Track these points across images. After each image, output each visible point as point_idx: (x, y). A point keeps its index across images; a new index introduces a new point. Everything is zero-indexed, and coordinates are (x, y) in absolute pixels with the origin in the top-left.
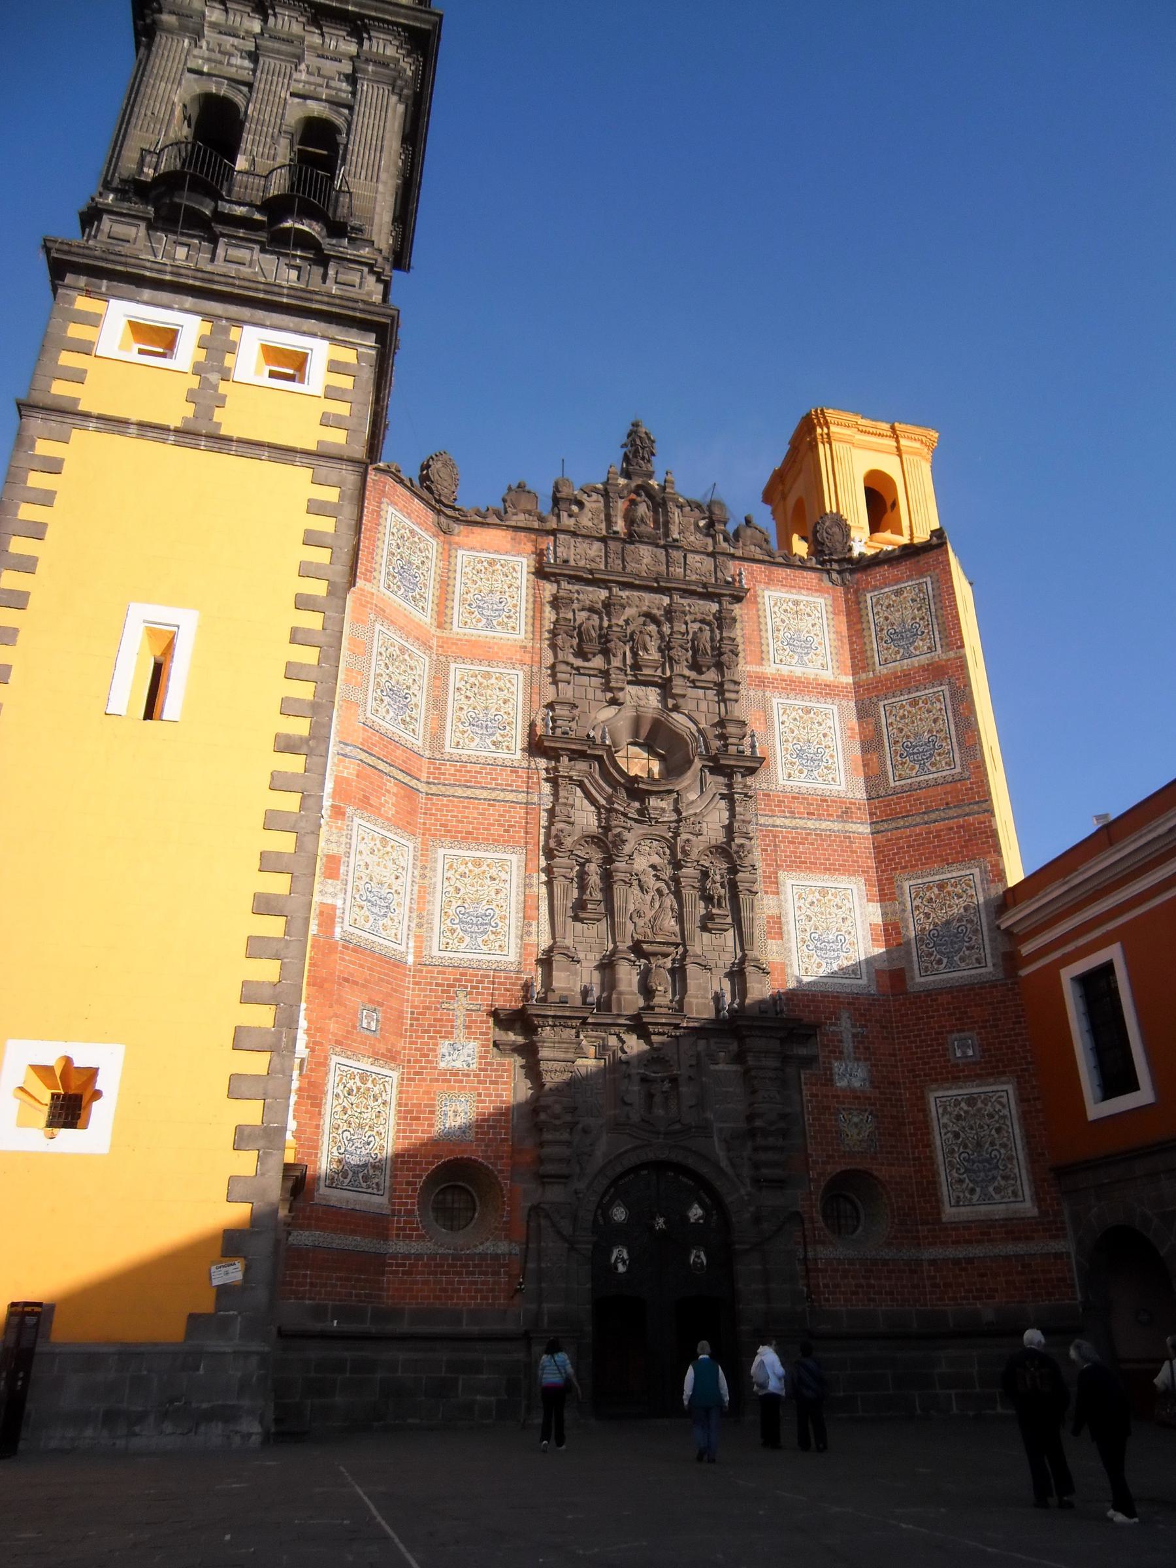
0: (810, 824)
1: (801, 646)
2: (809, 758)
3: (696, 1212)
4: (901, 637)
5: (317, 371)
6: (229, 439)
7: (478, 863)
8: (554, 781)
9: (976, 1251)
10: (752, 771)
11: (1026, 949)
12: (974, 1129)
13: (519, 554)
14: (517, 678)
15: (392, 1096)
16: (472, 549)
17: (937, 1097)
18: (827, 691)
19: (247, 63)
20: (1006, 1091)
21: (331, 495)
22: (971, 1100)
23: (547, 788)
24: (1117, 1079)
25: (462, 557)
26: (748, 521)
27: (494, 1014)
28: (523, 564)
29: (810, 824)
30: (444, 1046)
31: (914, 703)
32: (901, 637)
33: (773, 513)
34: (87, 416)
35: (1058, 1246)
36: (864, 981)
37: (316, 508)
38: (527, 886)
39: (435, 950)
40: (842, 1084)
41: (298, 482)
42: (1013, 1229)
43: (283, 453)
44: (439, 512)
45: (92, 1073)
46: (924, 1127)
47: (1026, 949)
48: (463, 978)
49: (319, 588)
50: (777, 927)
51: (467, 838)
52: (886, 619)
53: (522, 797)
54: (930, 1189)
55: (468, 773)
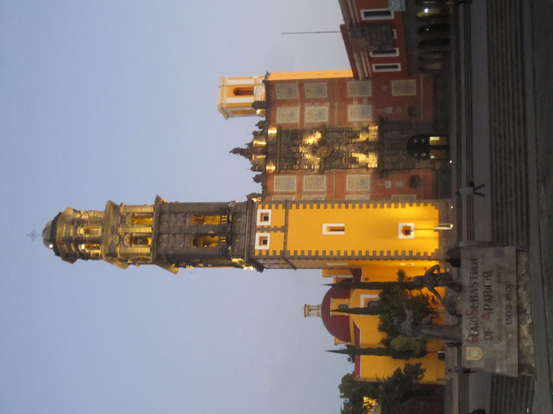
0: (336, 115)
1: (292, 115)
2: (320, 114)
3: (415, 141)
4: (290, 92)
5: (264, 211)
6: (285, 224)
7: (349, 183)
8: (331, 168)
9: (422, 90)
10: (325, 126)
11: (367, 75)
12: (400, 89)
13: (273, 179)
14: (305, 177)
15: (396, 195)
16: (273, 189)
17: (394, 94)
18: (302, 110)
19: (178, 236)
20: (394, 83)
21: (294, 206)
22: (395, 88)
23: (332, 170)
24: (396, 67)
25: (275, 190)
26: (256, 125)
27: (381, 177)
28: (276, 177)
29: (336, 115)
30: (387, 187)
31: (308, 91)
32: (290, 92)
33: (232, 117)
34: (284, 248)
35: (421, 77)
36: (370, 106)
37: (298, 207)
38: (353, 173)
39: (369, 189)
40: (391, 112)
41: (293, 211)
42: (418, 84)
43: (287, 214)
44: (266, 196)
45: (403, 227)
46: (400, 97)
47: (367, 75)
48: (373, 184)
49: (315, 206)
50: (360, 123)
51: (344, 185)
53: (334, 175)
54: (411, 97)
55: (329, 185)
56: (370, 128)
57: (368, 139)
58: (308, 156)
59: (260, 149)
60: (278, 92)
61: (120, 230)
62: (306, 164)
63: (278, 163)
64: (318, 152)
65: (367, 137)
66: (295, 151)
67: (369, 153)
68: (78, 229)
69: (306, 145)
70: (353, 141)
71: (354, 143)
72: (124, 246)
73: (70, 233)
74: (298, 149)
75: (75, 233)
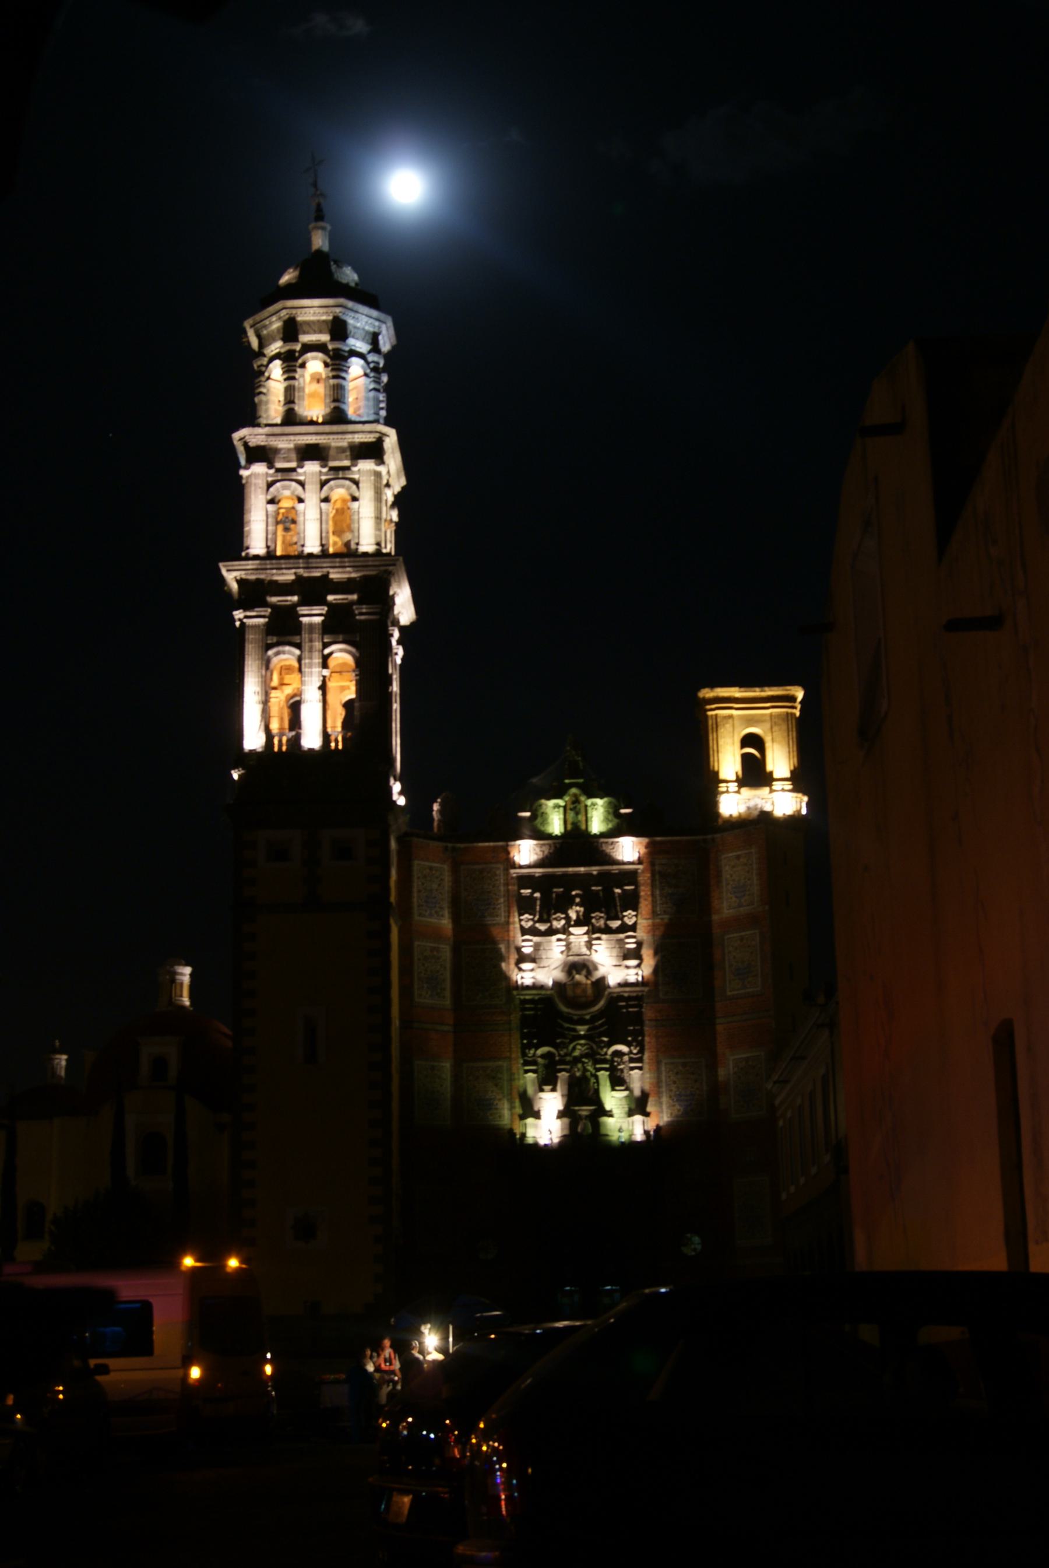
52: (731, 876)
56: (638, 1118)
57: (609, 1114)
58: (555, 951)
59: (584, 819)
60: (738, 857)
61: (312, 468)
62: (537, 947)
63: (538, 871)
64: (577, 977)
65: (615, 1112)
66: (573, 915)
67: (566, 1120)
68: (320, 355)
69: (589, 945)
70: (604, 1075)
71: (597, 1077)
72: (270, 485)
73: (305, 333)
74: (578, 923)
75: (308, 348)
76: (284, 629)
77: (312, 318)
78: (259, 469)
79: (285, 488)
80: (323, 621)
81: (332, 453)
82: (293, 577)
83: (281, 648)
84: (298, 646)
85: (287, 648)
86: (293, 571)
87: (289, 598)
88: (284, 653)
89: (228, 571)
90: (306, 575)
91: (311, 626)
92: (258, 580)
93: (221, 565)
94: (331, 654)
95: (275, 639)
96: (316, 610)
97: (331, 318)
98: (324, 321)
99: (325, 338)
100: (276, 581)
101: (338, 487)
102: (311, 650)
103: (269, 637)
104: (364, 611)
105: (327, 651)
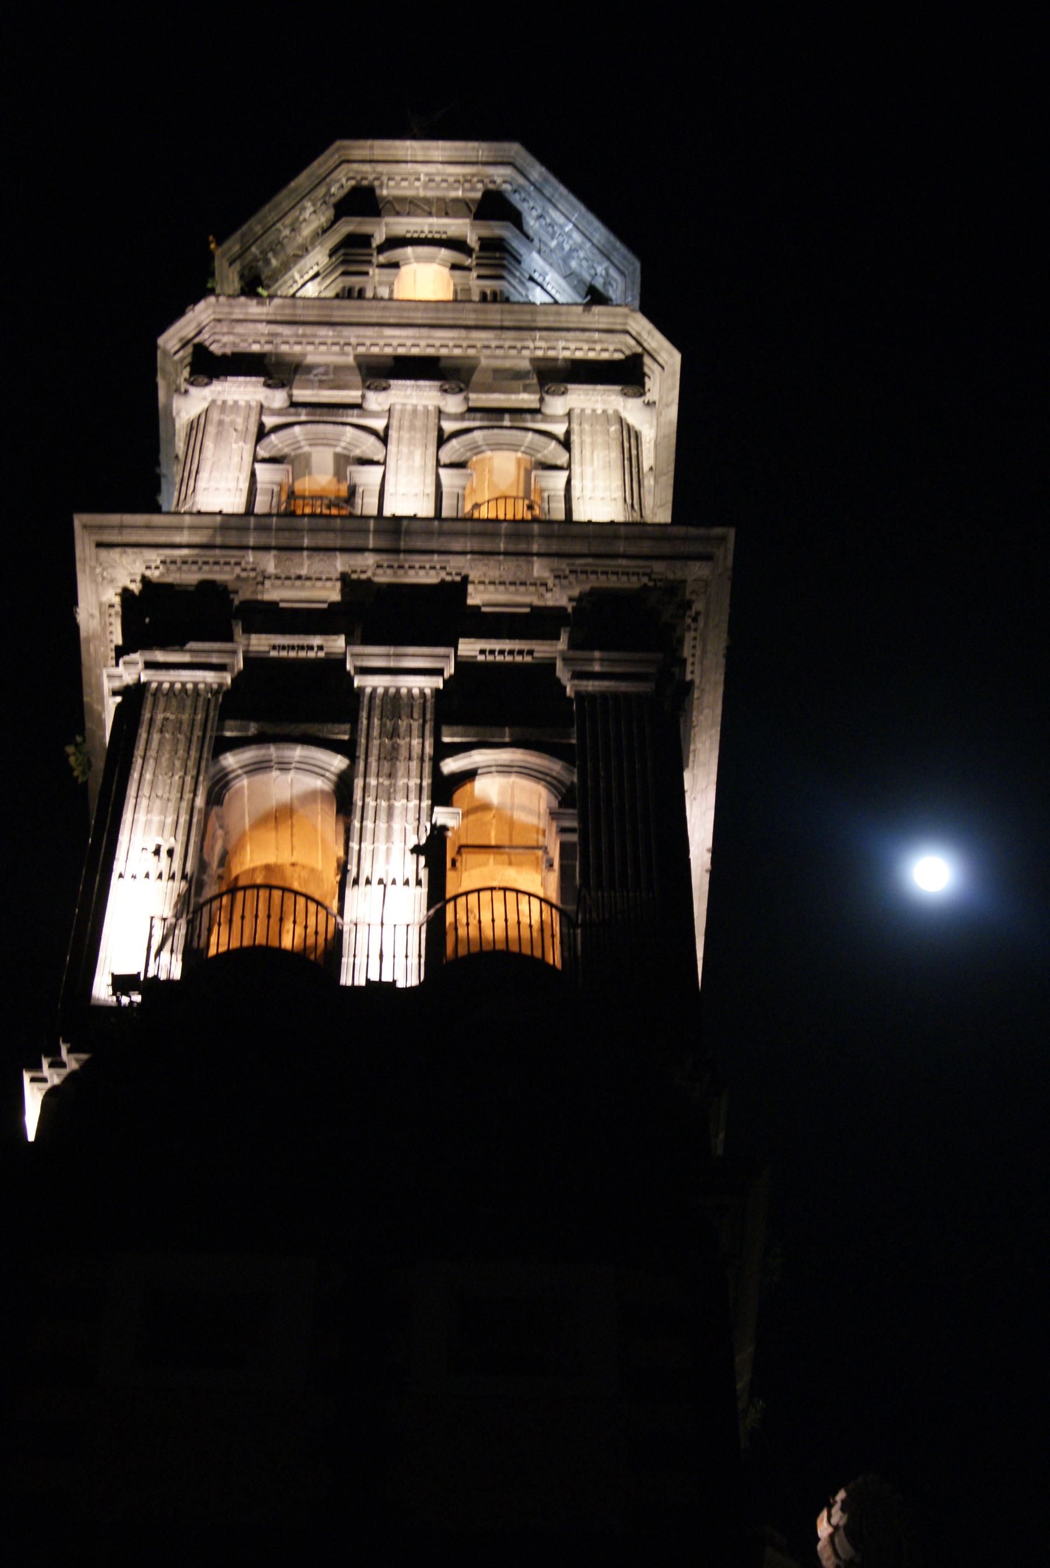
76: (294, 704)
77: (422, 193)
78: (242, 392)
79: (315, 442)
80: (437, 692)
81: (476, 378)
82: (334, 595)
83: (272, 751)
84: (347, 749)
85: (298, 752)
86: (340, 564)
87: (316, 641)
88: (284, 767)
89: (100, 545)
90: (383, 578)
91: (394, 705)
92: (207, 586)
93: (79, 520)
94: (470, 775)
95: (253, 729)
96: (416, 657)
97: (478, 195)
98: (465, 202)
99: (459, 227)
100: (274, 604)
101: (497, 447)
102: (391, 756)
103: (229, 723)
104: (597, 668)
105: (450, 765)
